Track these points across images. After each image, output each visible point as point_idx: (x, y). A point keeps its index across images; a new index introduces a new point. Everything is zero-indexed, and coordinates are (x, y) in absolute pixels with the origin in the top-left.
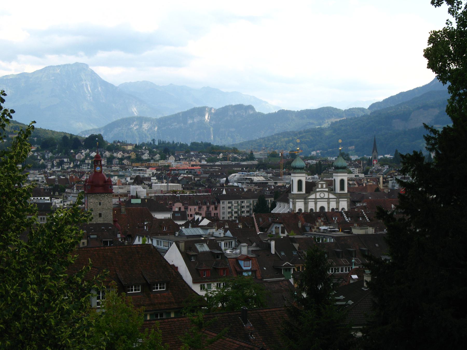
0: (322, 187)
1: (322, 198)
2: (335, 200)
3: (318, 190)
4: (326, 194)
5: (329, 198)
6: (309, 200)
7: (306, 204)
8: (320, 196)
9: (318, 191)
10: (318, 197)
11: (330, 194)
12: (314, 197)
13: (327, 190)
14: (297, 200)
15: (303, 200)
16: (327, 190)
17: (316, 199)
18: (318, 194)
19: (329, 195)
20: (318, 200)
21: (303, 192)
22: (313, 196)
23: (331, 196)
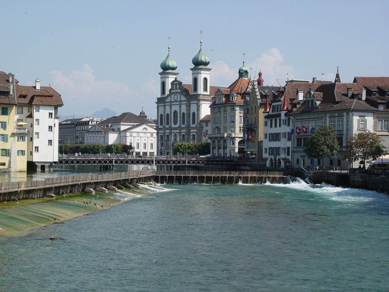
0: (176, 89)
1: (176, 101)
2: (185, 103)
3: (172, 91)
4: (179, 95)
5: (180, 101)
6: (166, 104)
8: (174, 100)
9: (174, 93)
10: (173, 100)
13: (179, 91)
16: (179, 91)
17: (171, 102)
18: (173, 96)
19: (180, 97)
20: (173, 103)
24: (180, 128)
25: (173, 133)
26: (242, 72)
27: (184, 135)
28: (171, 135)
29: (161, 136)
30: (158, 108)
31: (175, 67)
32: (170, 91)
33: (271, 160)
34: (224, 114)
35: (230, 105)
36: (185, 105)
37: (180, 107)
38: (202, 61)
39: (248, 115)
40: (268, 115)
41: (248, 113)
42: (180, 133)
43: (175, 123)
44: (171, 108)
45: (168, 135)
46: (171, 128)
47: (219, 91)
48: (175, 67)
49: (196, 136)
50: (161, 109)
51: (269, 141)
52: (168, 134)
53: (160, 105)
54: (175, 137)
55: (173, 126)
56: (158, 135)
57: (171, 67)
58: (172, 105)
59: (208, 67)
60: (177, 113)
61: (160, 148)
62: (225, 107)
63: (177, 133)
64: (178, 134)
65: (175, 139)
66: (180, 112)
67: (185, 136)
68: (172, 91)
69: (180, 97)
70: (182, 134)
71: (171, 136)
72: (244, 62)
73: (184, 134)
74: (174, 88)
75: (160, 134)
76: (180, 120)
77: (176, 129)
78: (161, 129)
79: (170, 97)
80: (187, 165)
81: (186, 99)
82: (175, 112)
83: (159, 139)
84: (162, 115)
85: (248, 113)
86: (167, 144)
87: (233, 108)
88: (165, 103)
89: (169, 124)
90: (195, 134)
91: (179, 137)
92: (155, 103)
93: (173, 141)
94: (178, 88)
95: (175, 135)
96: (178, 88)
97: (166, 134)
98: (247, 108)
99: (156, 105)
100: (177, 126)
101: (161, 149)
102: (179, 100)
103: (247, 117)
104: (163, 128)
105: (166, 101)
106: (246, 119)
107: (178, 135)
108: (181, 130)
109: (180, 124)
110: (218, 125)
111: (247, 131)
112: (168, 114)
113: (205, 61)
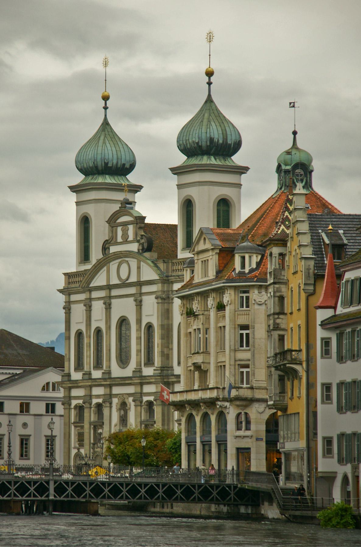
1: (124, 284)
3: (113, 249)
4: (134, 263)
5: (140, 284)
6: (95, 294)
9: (118, 255)
10: (115, 281)
11: (142, 263)
12: (104, 283)
17: (109, 287)
19: (139, 268)
20: (114, 292)
25: (116, 395)
26: (288, 167)
27: (150, 404)
28: (108, 405)
29: (80, 409)
30: (70, 310)
31: (127, 166)
32: (105, 248)
33: (345, 478)
34: (217, 320)
35: (235, 287)
36: (153, 296)
38: (211, 140)
39: (282, 321)
40: (335, 316)
41: (282, 313)
42: (138, 397)
44: (108, 307)
45: (99, 406)
47: (203, 238)
48: (127, 166)
50: (78, 311)
51: (340, 409)
52: (100, 401)
53: (74, 298)
54: (122, 412)
55: (117, 372)
56: (70, 405)
57: (110, 165)
58: (110, 297)
59: (238, 159)
60: (128, 324)
61: (74, 452)
62: (220, 291)
63: (130, 395)
64: (131, 399)
65: (124, 420)
66: (139, 321)
67: (155, 408)
68: (113, 249)
69: (139, 268)
70: (145, 399)
71: (111, 407)
72: (295, 133)
73: (151, 398)
74: (120, 239)
75: (74, 403)
76: (139, 351)
77: (123, 382)
78: (76, 384)
79: (105, 268)
80: (52, 497)
81: (157, 277)
82: (123, 321)
83: (73, 420)
84: (79, 334)
85: (282, 313)
86: (98, 438)
87: (245, 295)
88: (90, 290)
89: (102, 364)
91: (136, 411)
92: (60, 291)
93: (115, 426)
94: (131, 238)
95: (123, 406)
96: (131, 238)
97: (95, 401)
98: (278, 294)
99: (62, 298)
101: (78, 456)
103: (277, 327)
104: (83, 380)
105: (91, 285)
106: (276, 334)
107: (133, 404)
108: (141, 384)
109: (139, 364)
110: (199, 359)
111: (279, 376)
112: (98, 331)
113: (221, 141)
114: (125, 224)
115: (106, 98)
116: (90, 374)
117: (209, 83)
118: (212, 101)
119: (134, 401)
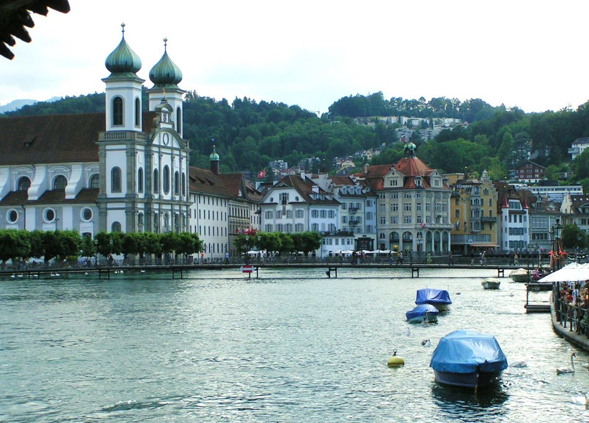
0: (164, 122)
1: (165, 147)
4: (170, 136)
5: (172, 148)
7: (148, 156)
8: (165, 144)
10: (162, 144)
11: (174, 138)
14: (138, 147)
15: (142, 148)
16: (170, 126)
17: (159, 146)
21: (139, 127)
22: (156, 142)
23: (176, 145)
24: (171, 202)
25: (164, 209)
29: (140, 215)
37: (172, 160)
43: (166, 191)
44: (160, 159)
46: (161, 202)
49: (186, 219)
64: (170, 213)
76: (172, 185)
77: (167, 202)
79: (158, 135)
90: (185, 214)
95: (166, 215)
96: (167, 121)
100: (167, 197)
102: (169, 145)
109: (172, 194)
112: (156, 171)
114: (165, 112)
115: (123, 26)
116: (154, 196)
117: (165, 45)
118: (167, 54)
119: (172, 215)
